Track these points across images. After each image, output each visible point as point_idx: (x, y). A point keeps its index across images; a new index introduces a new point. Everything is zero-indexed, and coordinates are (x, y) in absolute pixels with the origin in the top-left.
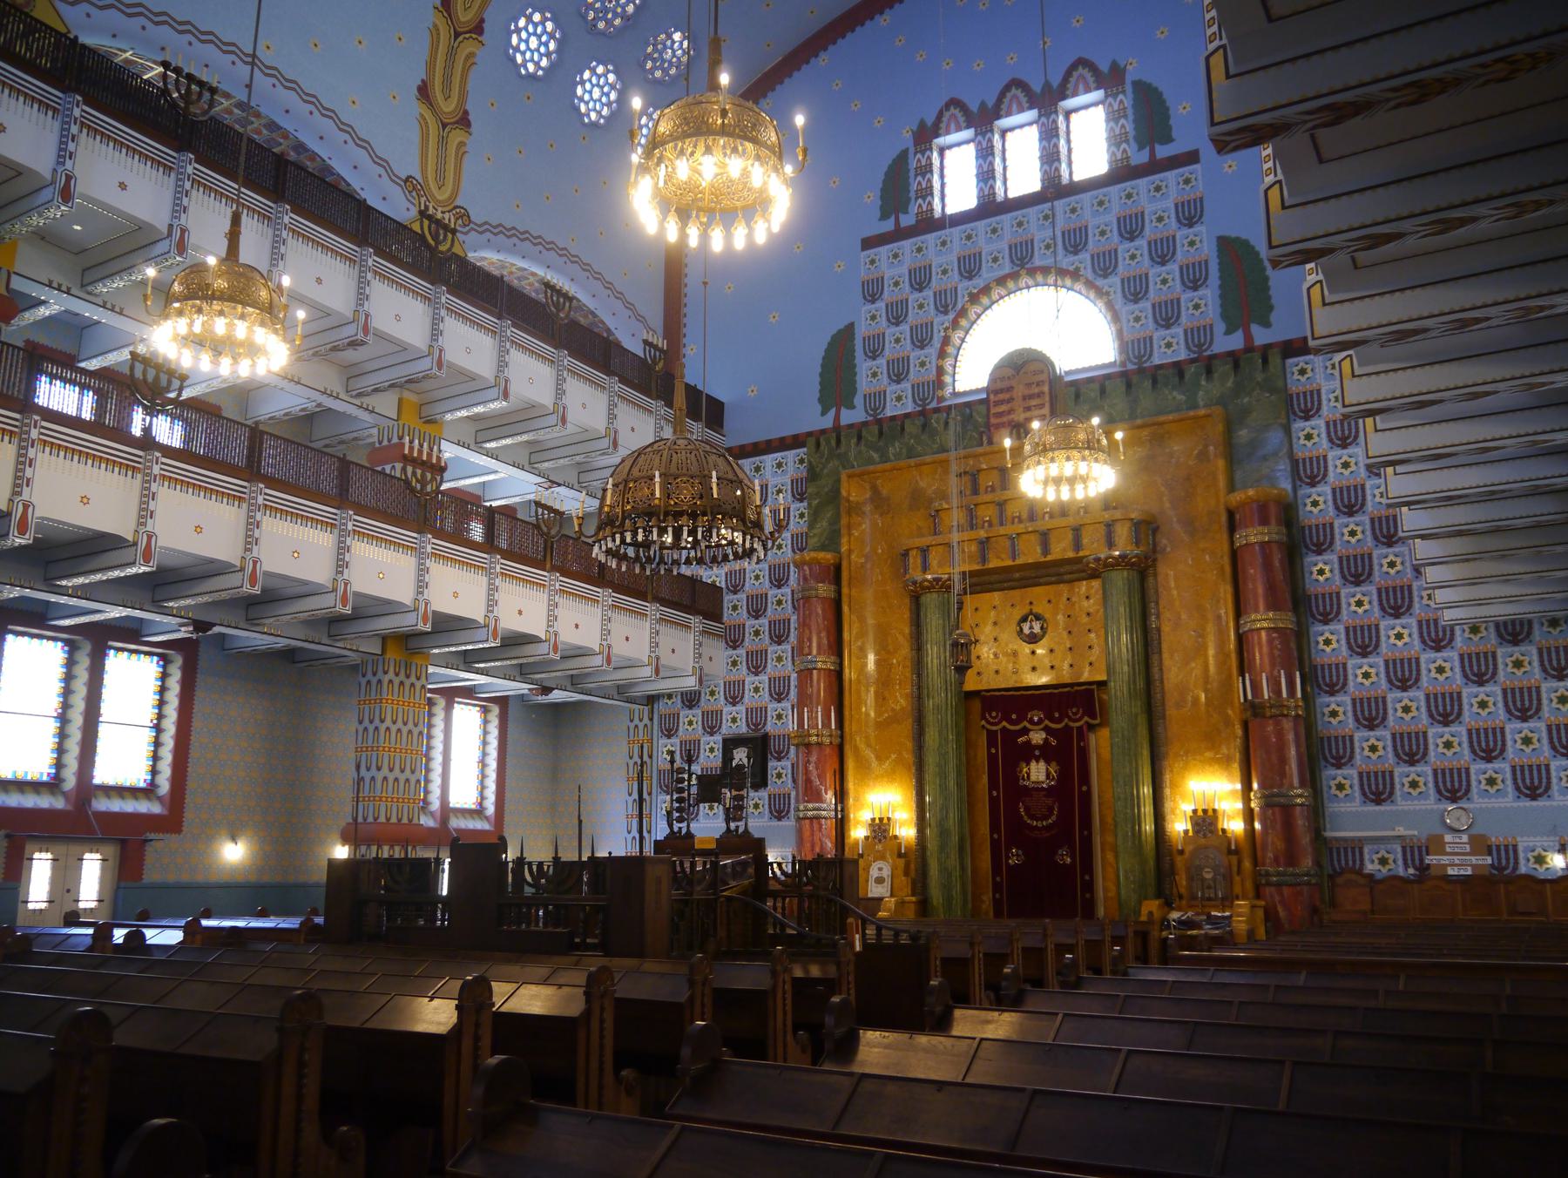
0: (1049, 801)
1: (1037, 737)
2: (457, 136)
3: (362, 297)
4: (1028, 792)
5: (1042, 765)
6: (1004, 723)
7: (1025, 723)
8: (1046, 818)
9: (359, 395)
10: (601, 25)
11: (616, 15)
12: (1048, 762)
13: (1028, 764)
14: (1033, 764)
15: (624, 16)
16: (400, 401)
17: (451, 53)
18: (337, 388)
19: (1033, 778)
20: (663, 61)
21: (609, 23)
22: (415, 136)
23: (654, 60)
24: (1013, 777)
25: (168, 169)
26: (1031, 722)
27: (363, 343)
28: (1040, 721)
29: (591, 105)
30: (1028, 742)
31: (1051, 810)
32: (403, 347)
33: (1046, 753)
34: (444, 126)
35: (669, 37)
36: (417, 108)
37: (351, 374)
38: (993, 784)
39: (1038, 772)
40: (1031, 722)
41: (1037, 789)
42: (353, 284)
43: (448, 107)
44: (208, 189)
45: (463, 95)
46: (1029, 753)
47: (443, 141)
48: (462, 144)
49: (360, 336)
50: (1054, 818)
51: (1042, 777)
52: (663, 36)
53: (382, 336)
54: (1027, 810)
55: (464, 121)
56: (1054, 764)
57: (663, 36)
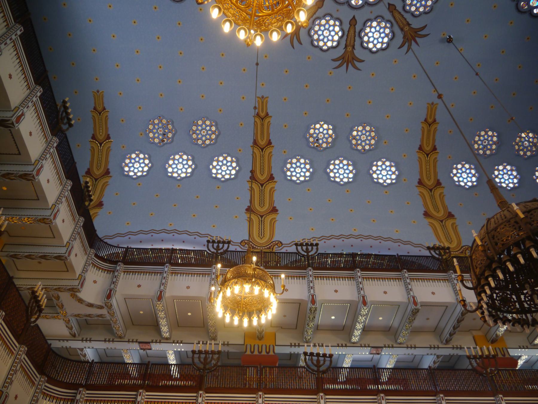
2: (449, 223)
3: (408, 290)
9: (447, 342)
10: (488, 152)
11: (491, 145)
15: (494, 143)
16: (474, 337)
17: (432, 197)
18: (436, 343)
20: (527, 147)
21: (491, 150)
22: (430, 230)
23: (522, 150)
25: (303, 277)
27: (417, 311)
29: (507, 182)
32: (446, 306)
34: (442, 221)
35: (521, 137)
36: (427, 221)
37: (436, 331)
42: (403, 288)
43: (441, 214)
44: (322, 278)
45: (445, 207)
47: (444, 227)
48: (453, 224)
49: (414, 307)
52: (518, 139)
53: (425, 305)
55: (450, 216)
57: (518, 139)
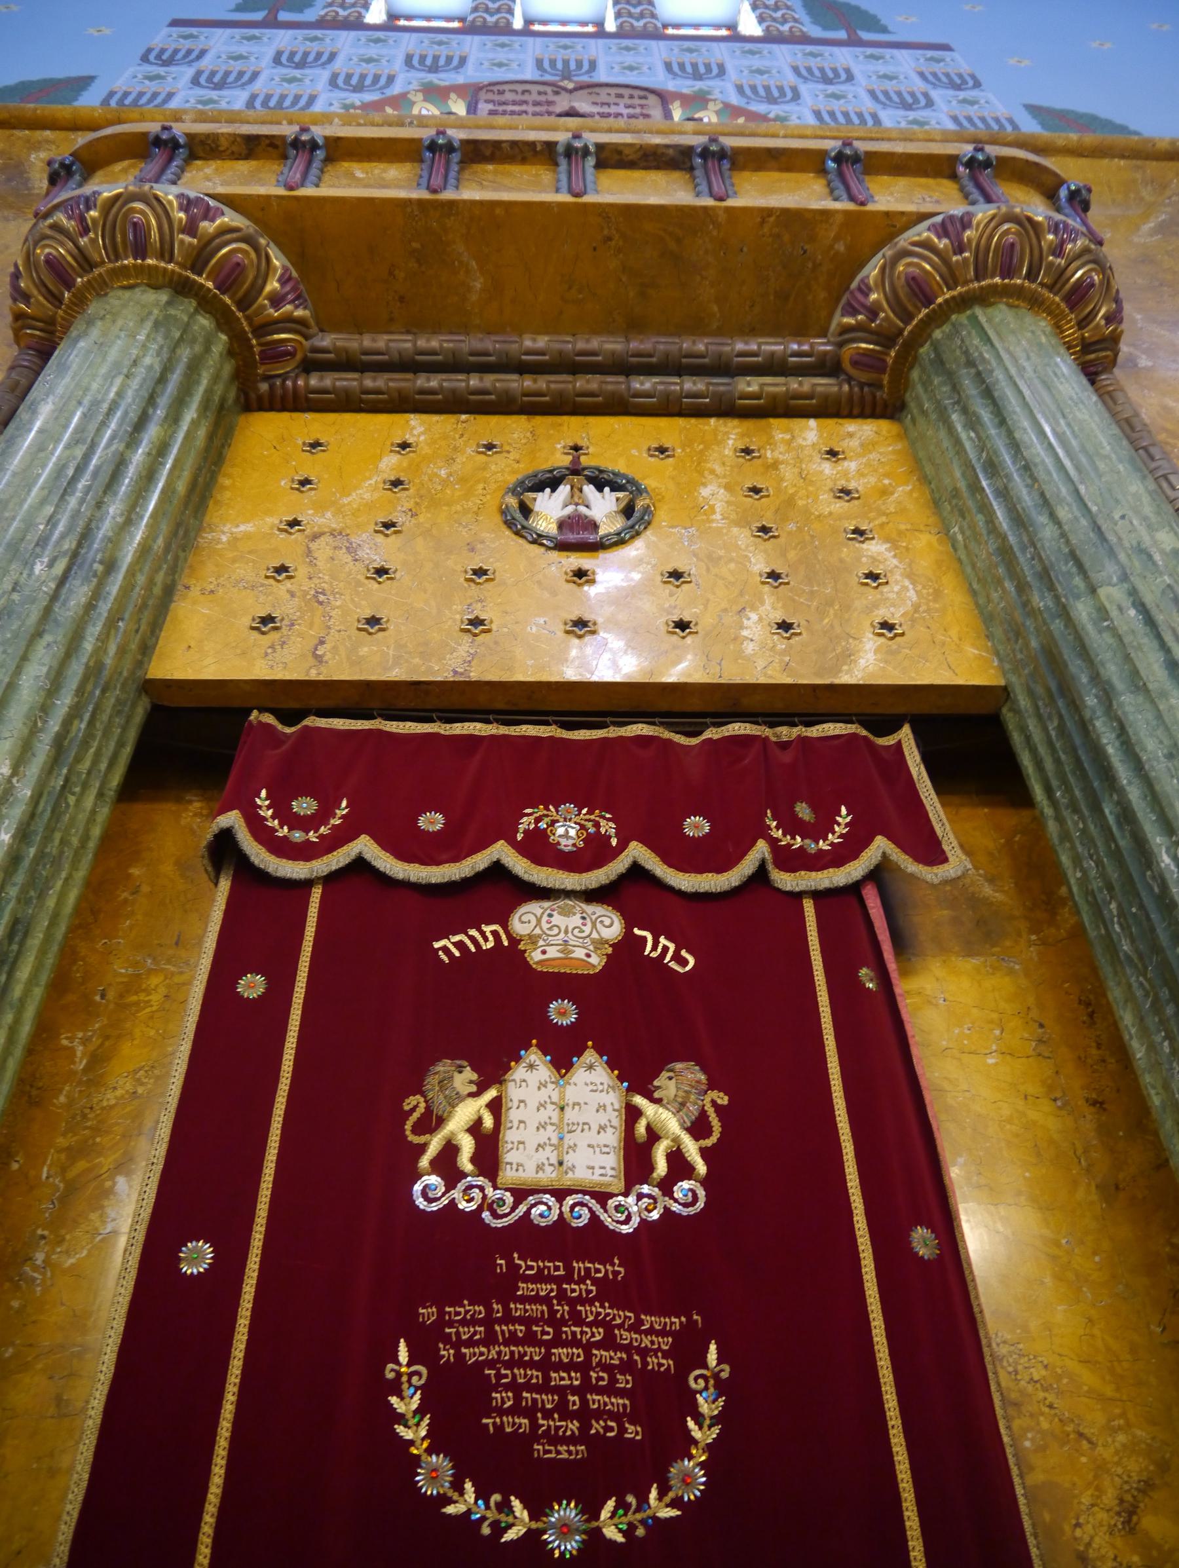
0: (653, 1336)
1: (567, 934)
4: (473, 1256)
5: (593, 1084)
6: (365, 846)
7: (501, 852)
8: (589, 1484)
12: (637, 1076)
13: (492, 1073)
14: (530, 1077)
19: (524, 1159)
24: (357, 1128)
26: (538, 847)
28: (595, 851)
30: (511, 955)
31: (663, 1402)
33: (625, 1020)
38: (197, 1190)
39: (559, 1132)
40: (538, 847)
41: (560, 1241)
46: (503, 1016)
50: (691, 1474)
51: (596, 1160)
54: (456, 1400)
56: (680, 1081)
